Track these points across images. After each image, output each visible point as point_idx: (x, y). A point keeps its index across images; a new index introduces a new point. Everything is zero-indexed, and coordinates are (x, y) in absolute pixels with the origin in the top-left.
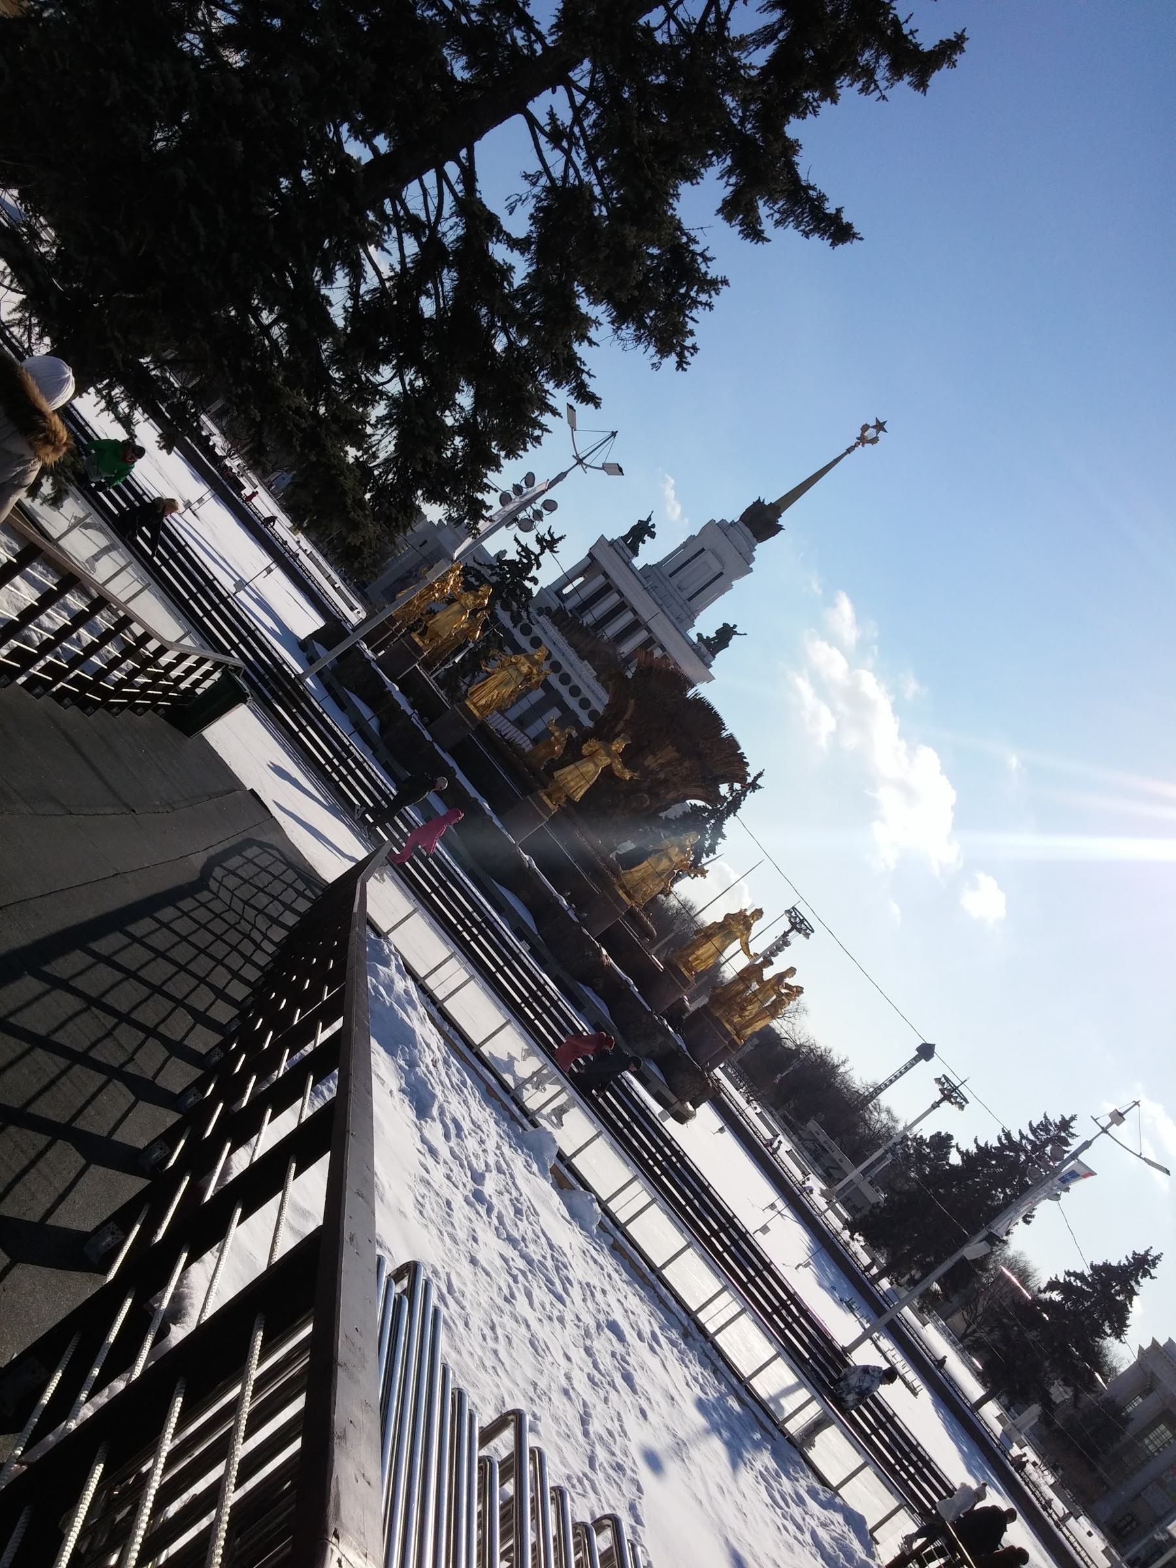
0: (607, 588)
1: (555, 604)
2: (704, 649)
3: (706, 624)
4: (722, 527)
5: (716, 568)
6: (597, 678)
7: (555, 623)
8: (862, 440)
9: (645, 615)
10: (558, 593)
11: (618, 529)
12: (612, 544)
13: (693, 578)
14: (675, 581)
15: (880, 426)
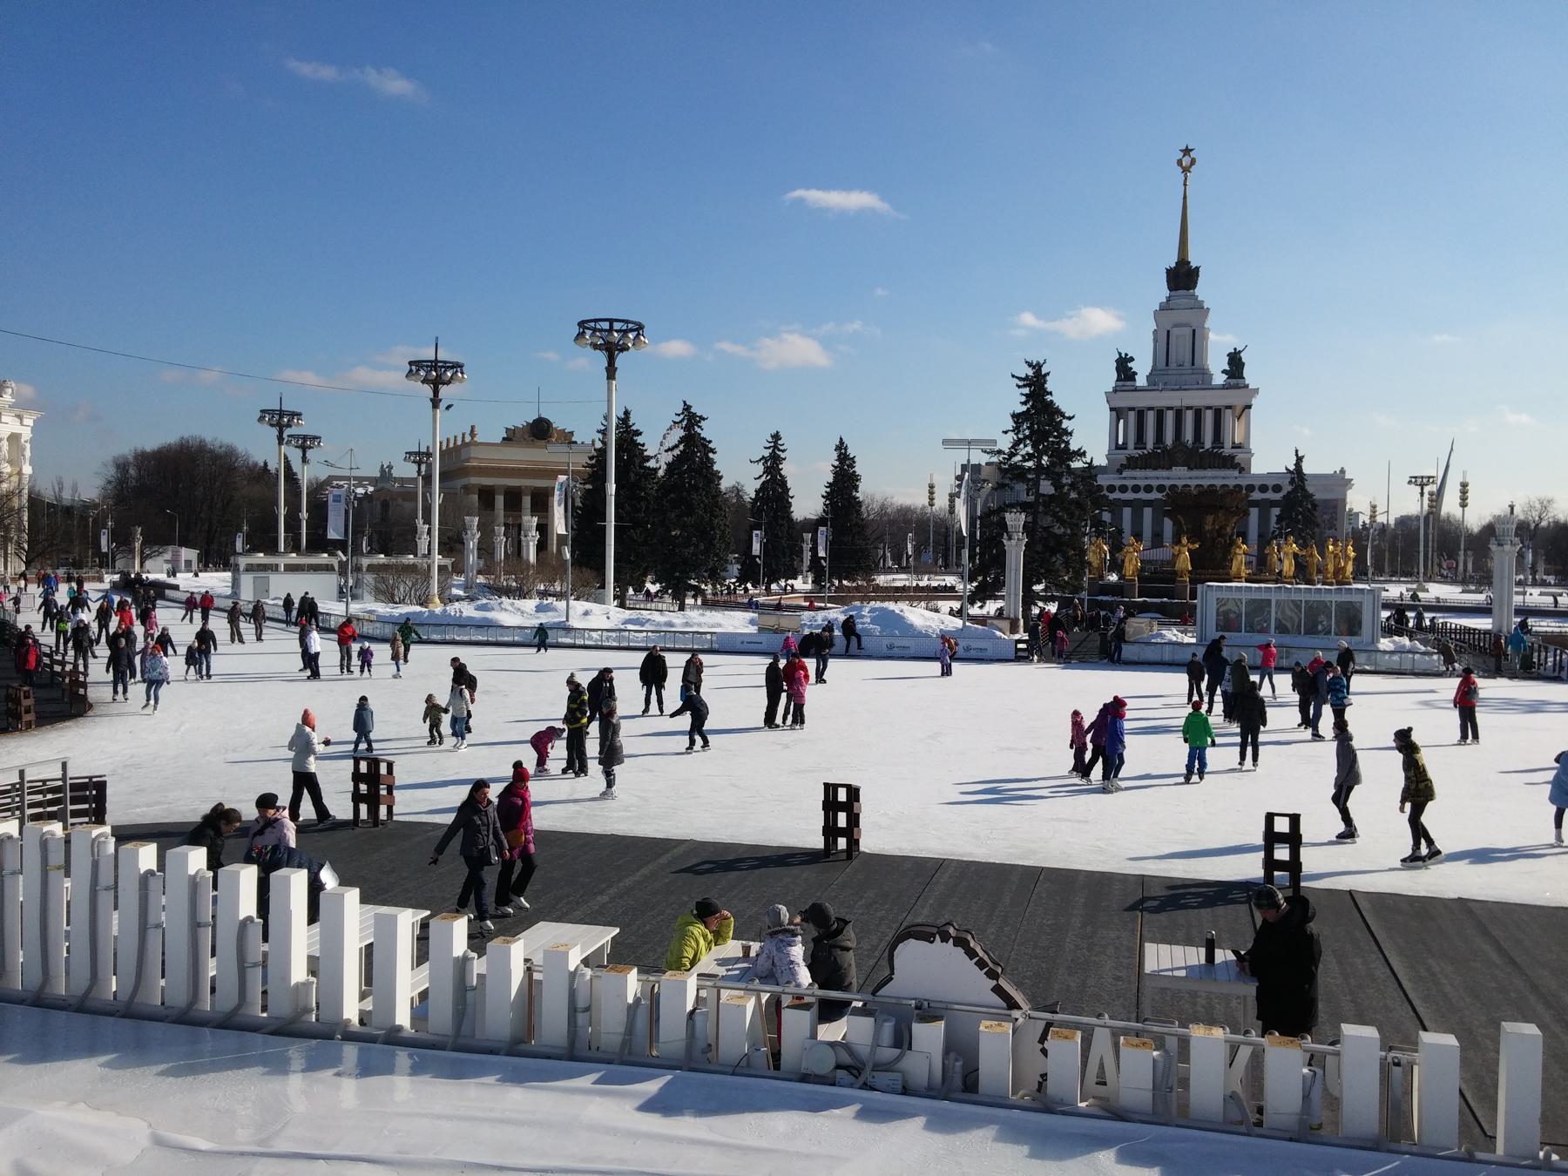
0: (1141, 414)
1: (1122, 456)
2: (1233, 381)
3: (1217, 366)
4: (1164, 307)
5: (1188, 331)
6: (1190, 468)
7: (1135, 468)
8: (1186, 170)
9: (1176, 403)
10: (1118, 447)
11: (1110, 378)
12: (1115, 390)
13: (1181, 351)
14: (1173, 365)
15: (1187, 151)
